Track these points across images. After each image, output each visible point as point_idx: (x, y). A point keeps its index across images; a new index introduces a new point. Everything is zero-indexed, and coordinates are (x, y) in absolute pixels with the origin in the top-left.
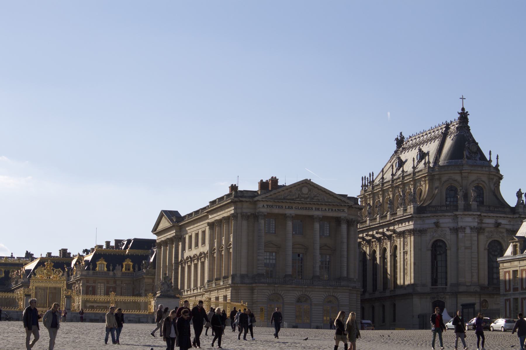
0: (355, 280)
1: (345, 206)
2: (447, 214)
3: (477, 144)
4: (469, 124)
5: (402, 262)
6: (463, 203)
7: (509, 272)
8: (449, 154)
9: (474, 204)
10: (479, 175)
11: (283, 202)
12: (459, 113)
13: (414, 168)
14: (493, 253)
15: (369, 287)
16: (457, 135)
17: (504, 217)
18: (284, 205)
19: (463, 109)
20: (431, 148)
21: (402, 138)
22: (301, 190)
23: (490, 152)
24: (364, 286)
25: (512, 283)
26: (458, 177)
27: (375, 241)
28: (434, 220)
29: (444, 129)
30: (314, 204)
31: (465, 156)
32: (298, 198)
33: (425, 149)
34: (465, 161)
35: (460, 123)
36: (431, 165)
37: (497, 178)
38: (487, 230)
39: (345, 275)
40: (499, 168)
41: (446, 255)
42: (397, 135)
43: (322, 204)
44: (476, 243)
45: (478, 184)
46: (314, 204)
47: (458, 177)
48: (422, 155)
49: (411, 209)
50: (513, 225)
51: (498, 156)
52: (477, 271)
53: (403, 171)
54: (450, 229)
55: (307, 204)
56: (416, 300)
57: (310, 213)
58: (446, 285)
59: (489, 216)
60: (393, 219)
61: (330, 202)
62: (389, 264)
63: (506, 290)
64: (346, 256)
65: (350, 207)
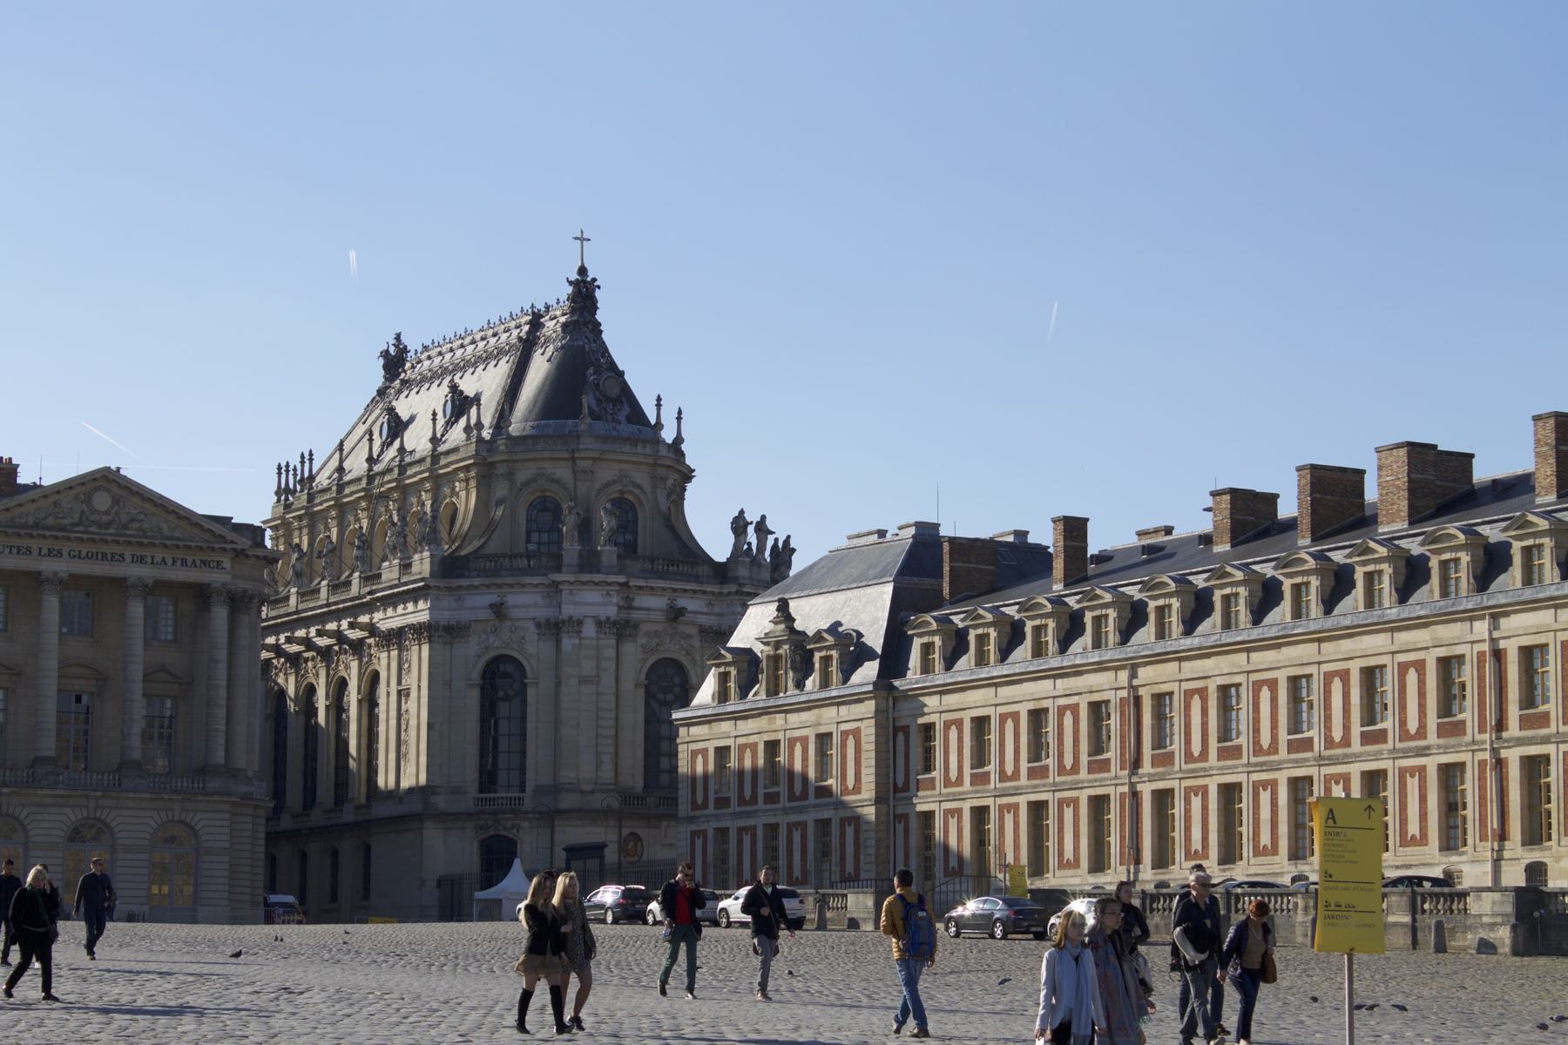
0: (250, 773)
1: (225, 550)
2: (528, 580)
3: (621, 374)
4: (599, 316)
5: (393, 723)
6: (577, 547)
7: (704, 752)
9: (608, 553)
10: (623, 466)
11: (31, 536)
12: (571, 283)
13: (435, 441)
14: (661, 696)
15: (294, 796)
16: (563, 347)
17: (695, 592)
18: (34, 544)
19: (582, 271)
20: (487, 383)
21: (402, 351)
22: (88, 500)
23: (659, 399)
24: (278, 793)
25: (712, 786)
26: (563, 472)
27: (313, 659)
28: (493, 598)
29: (526, 328)
30: (130, 543)
31: (586, 411)
32: (80, 523)
33: (468, 385)
34: (585, 423)
35: (573, 311)
36: (486, 434)
37: (677, 476)
38: (644, 627)
39: (219, 757)
40: (684, 447)
41: (524, 702)
42: (385, 341)
43: (154, 545)
44: (613, 665)
45: (622, 492)
46: (130, 543)
47: (563, 472)
48: (461, 404)
49: (422, 564)
50: (720, 615)
51: (680, 412)
52: (612, 749)
53: (402, 450)
54: (538, 625)
55: (106, 542)
56: (433, 836)
57: (117, 570)
58: (522, 789)
60: (370, 593)
61: (178, 539)
62: (353, 727)
63: (695, 806)
64: (223, 702)
65: (239, 554)
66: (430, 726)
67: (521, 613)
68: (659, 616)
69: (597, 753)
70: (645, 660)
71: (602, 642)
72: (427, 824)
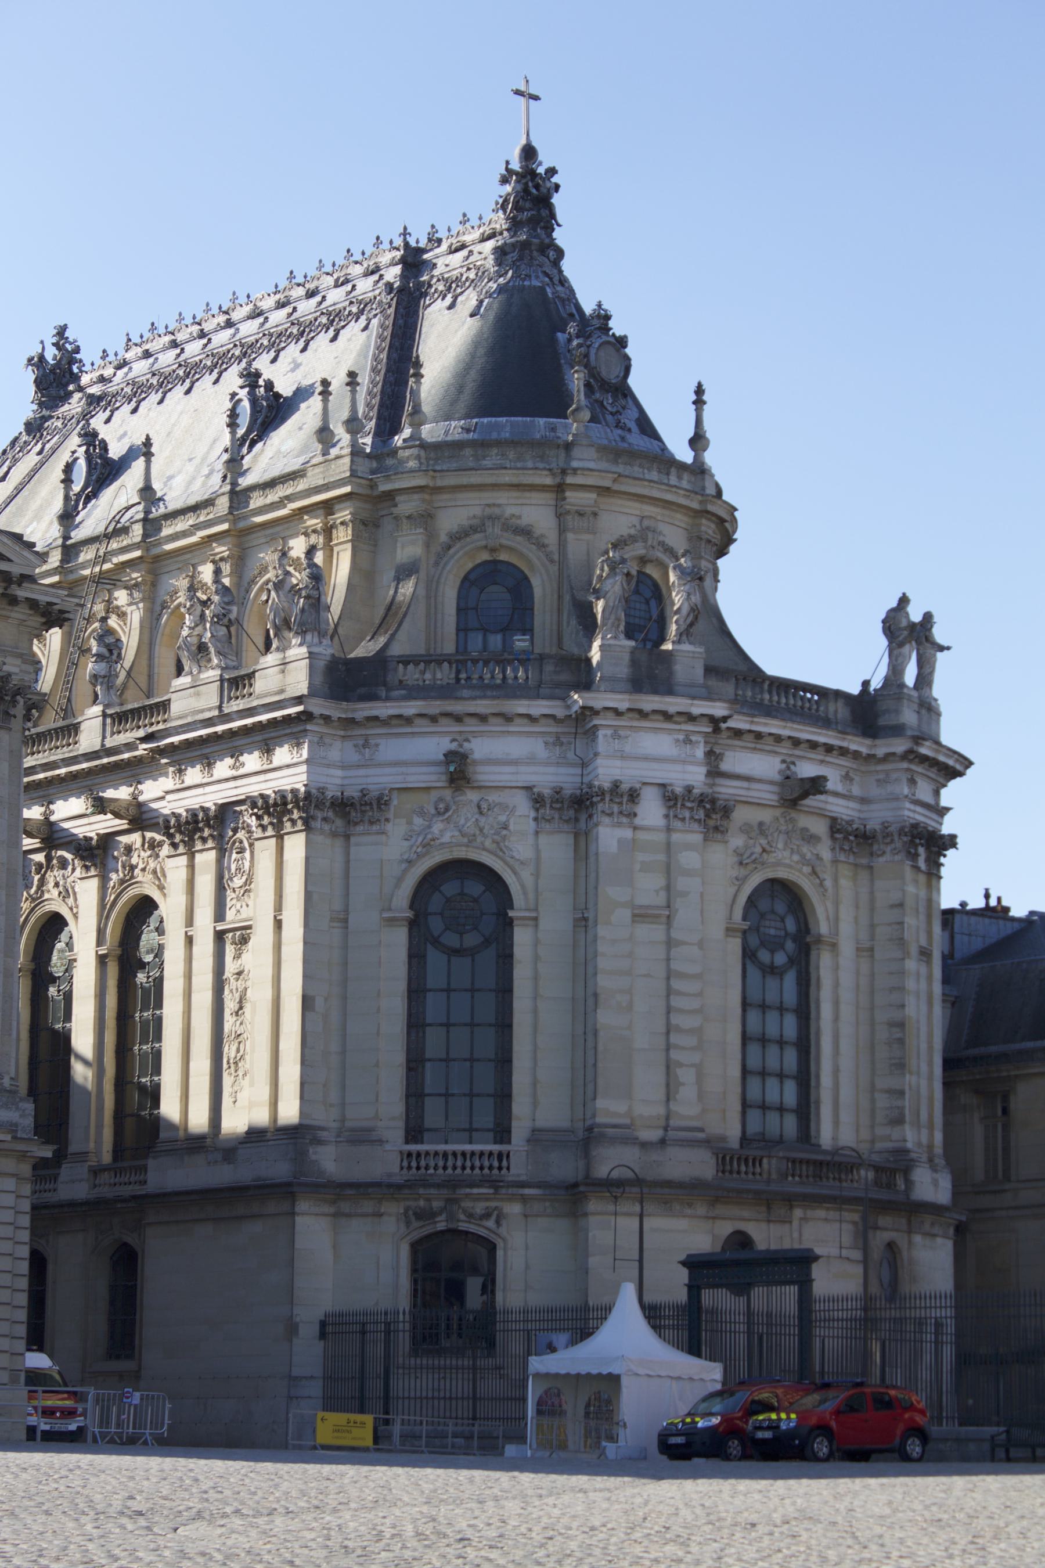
2: (521, 706)
8: (470, 386)
16: (501, 289)
17: (829, 749)
26: (537, 513)
34: (572, 427)
38: (741, 815)
41: (506, 958)
45: (643, 560)
47: (537, 513)
49: (285, 673)
50: (863, 800)
53: (147, 491)
54: (537, 801)
56: (313, 1228)
59: (759, 736)
60: (148, 738)
66: (307, 1003)
67: (503, 775)
68: (767, 794)
69: (669, 1067)
70: (742, 881)
71: (676, 837)
72: (302, 1206)
